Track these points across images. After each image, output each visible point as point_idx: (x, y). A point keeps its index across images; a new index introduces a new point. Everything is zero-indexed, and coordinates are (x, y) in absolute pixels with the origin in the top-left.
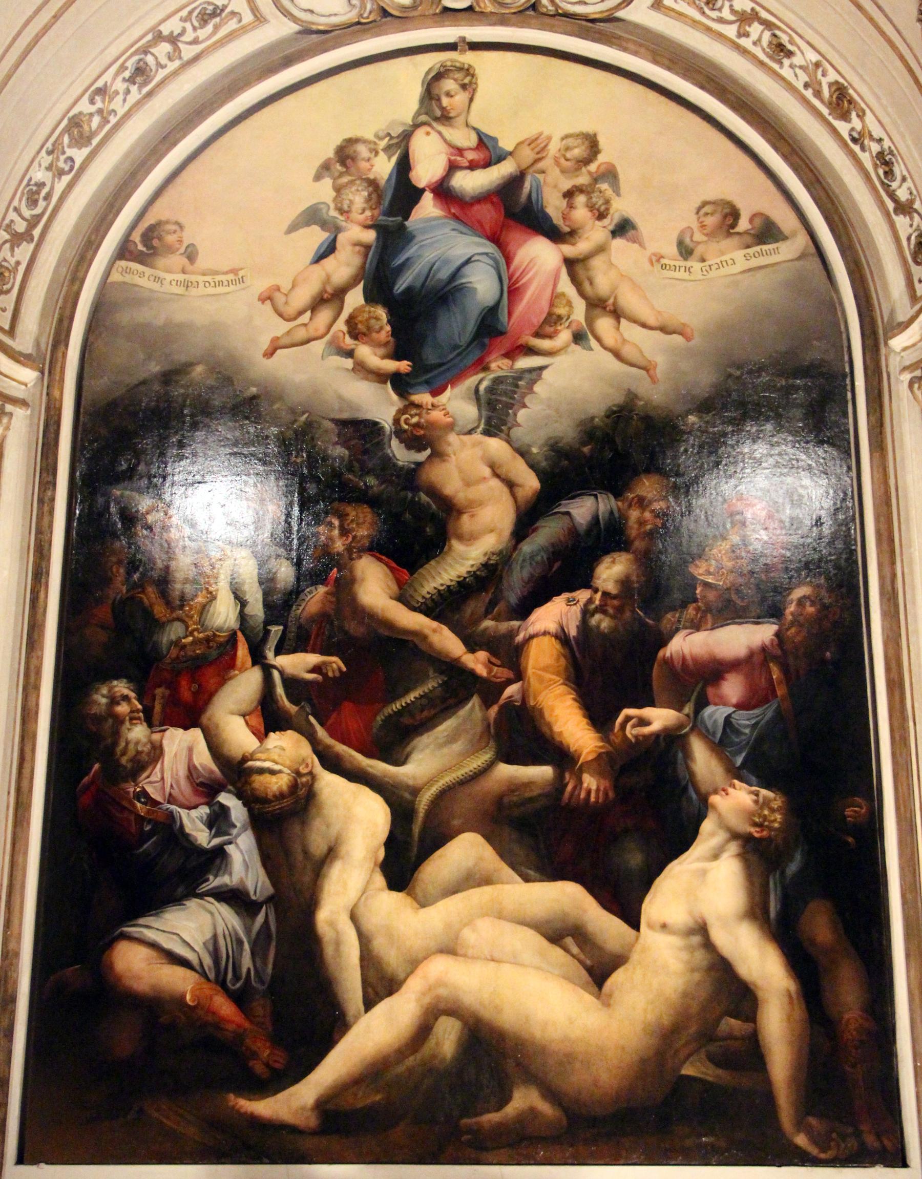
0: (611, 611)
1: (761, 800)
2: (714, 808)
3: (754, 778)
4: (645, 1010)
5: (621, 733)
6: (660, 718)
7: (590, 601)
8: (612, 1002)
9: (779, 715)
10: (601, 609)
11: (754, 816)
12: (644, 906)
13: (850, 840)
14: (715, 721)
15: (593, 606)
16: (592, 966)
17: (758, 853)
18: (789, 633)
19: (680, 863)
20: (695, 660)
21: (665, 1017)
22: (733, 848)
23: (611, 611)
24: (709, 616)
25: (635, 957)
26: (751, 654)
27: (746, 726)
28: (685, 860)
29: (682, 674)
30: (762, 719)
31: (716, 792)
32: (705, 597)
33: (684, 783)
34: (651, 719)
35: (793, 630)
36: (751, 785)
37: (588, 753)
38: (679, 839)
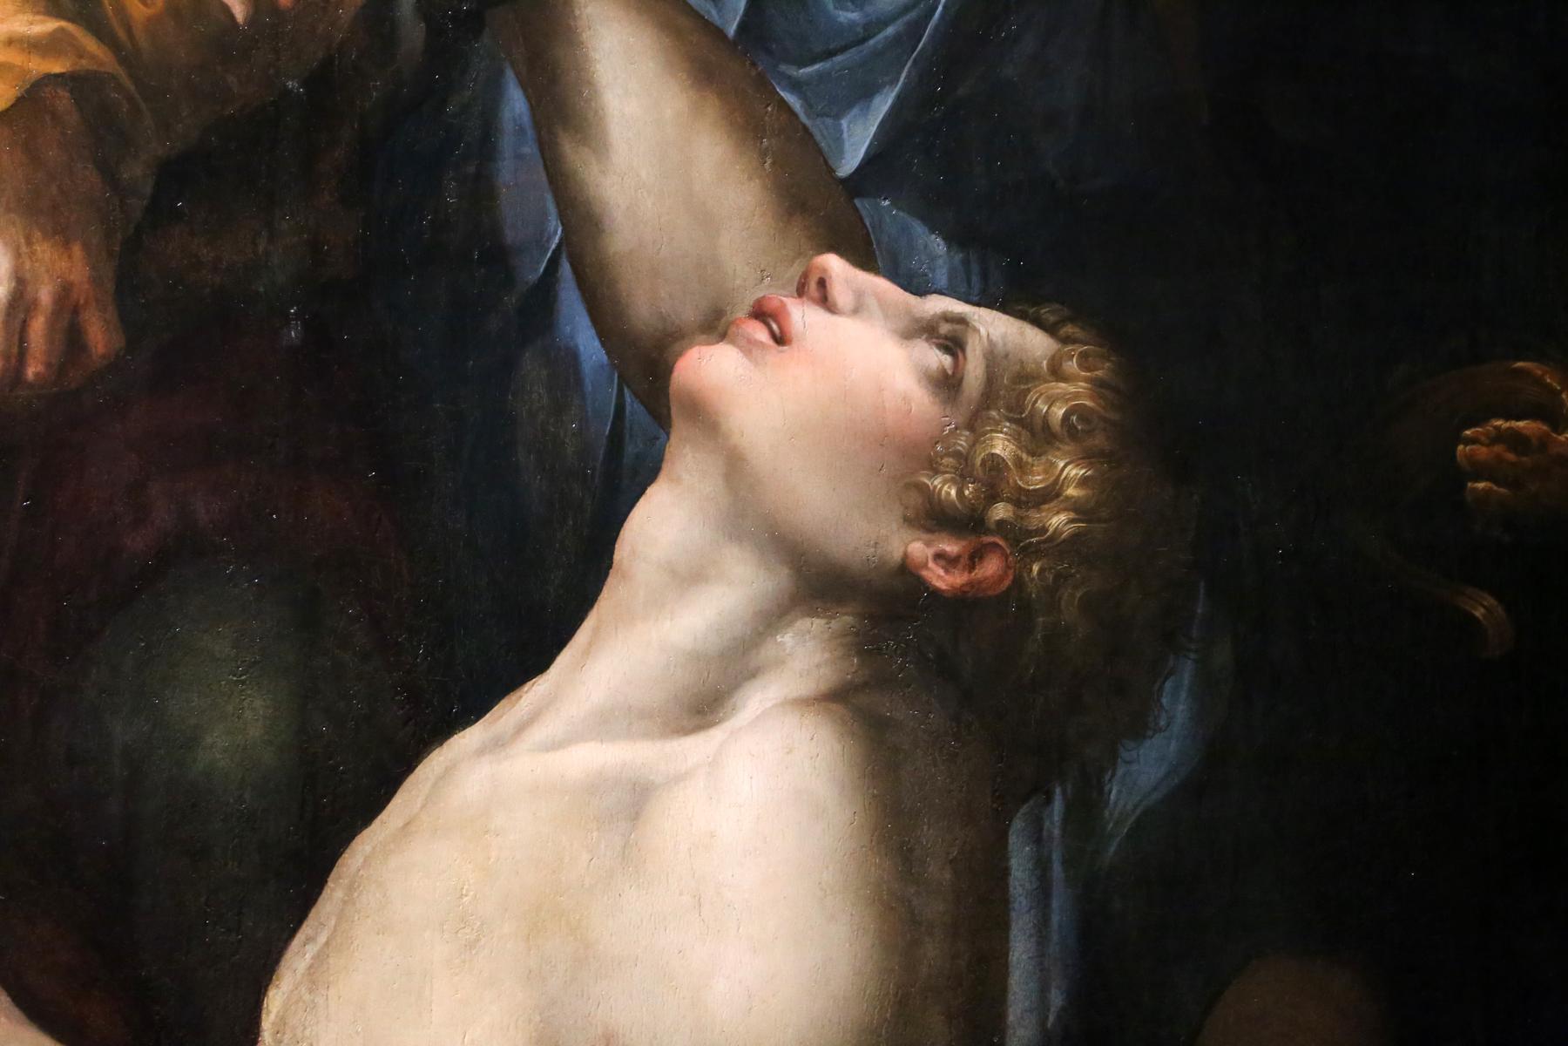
2: (704, 416)
3: (938, 245)
12: (275, 1002)
13: (1482, 607)
17: (942, 674)
19: (498, 745)
22: (806, 654)
28: (522, 728)
31: (716, 327)
33: (533, 272)
36: (917, 286)
38: (500, 607)
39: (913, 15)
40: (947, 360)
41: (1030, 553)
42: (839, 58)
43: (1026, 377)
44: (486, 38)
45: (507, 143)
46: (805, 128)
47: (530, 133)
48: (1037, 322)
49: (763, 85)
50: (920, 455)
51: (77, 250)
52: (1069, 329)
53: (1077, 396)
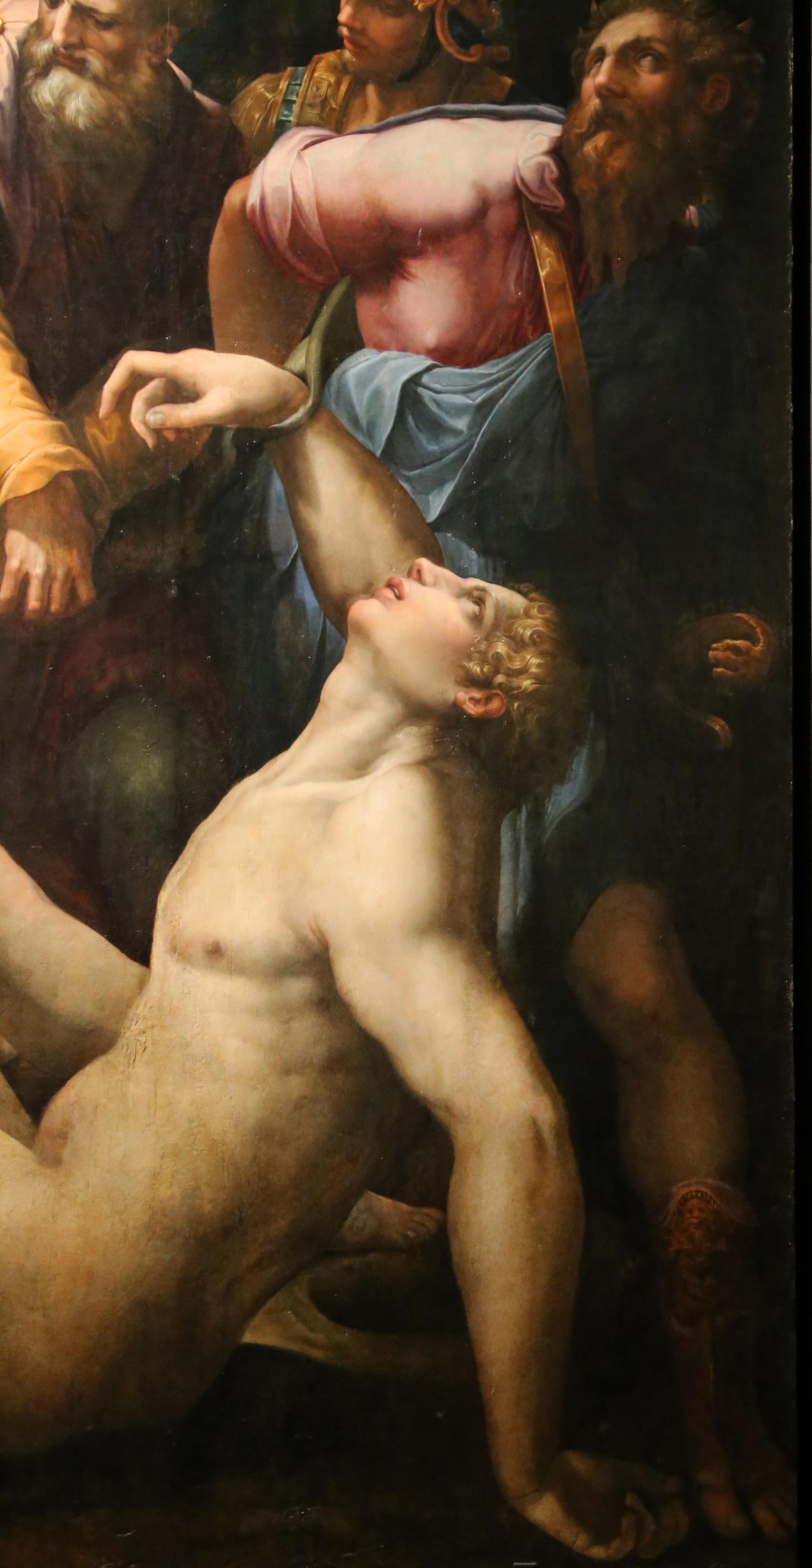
0: (96, 64)
1: (489, 613)
2: (364, 633)
3: (473, 554)
4: (155, 1175)
5: (116, 422)
6: (226, 379)
7: (39, 29)
8: (66, 1154)
9: (549, 383)
10: (69, 58)
11: (470, 659)
12: (163, 897)
13: (718, 725)
14: (377, 395)
15: (43, 49)
16: (16, 1060)
18: (588, 148)
19: (266, 783)
20: (324, 216)
21: (207, 1193)
22: (410, 743)
23: (96, 64)
24: (371, 91)
25: (131, 1031)
26: (483, 206)
27: (459, 411)
28: (277, 775)
29: (289, 255)
30: (503, 391)
31: (369, 591)
32: (363, 32)
33: (284, 564)
34: (201, 385)
35: (600, 140)
36: (463, 573)
37: (24, 474)
38: (270, 720)
39: (463, 448)
40: (476, 608)
41: (515, 698)
42: (428, 467)
43: (513, 617)
44: (264, 457)
45: (273, 504)
46: (412, 499)
47: (284, 499)
48: (519, 591)
49: (392, 478)
50: (465, 652)
51: (75, 552)
52: (533, 595)
53: (536, 626)
